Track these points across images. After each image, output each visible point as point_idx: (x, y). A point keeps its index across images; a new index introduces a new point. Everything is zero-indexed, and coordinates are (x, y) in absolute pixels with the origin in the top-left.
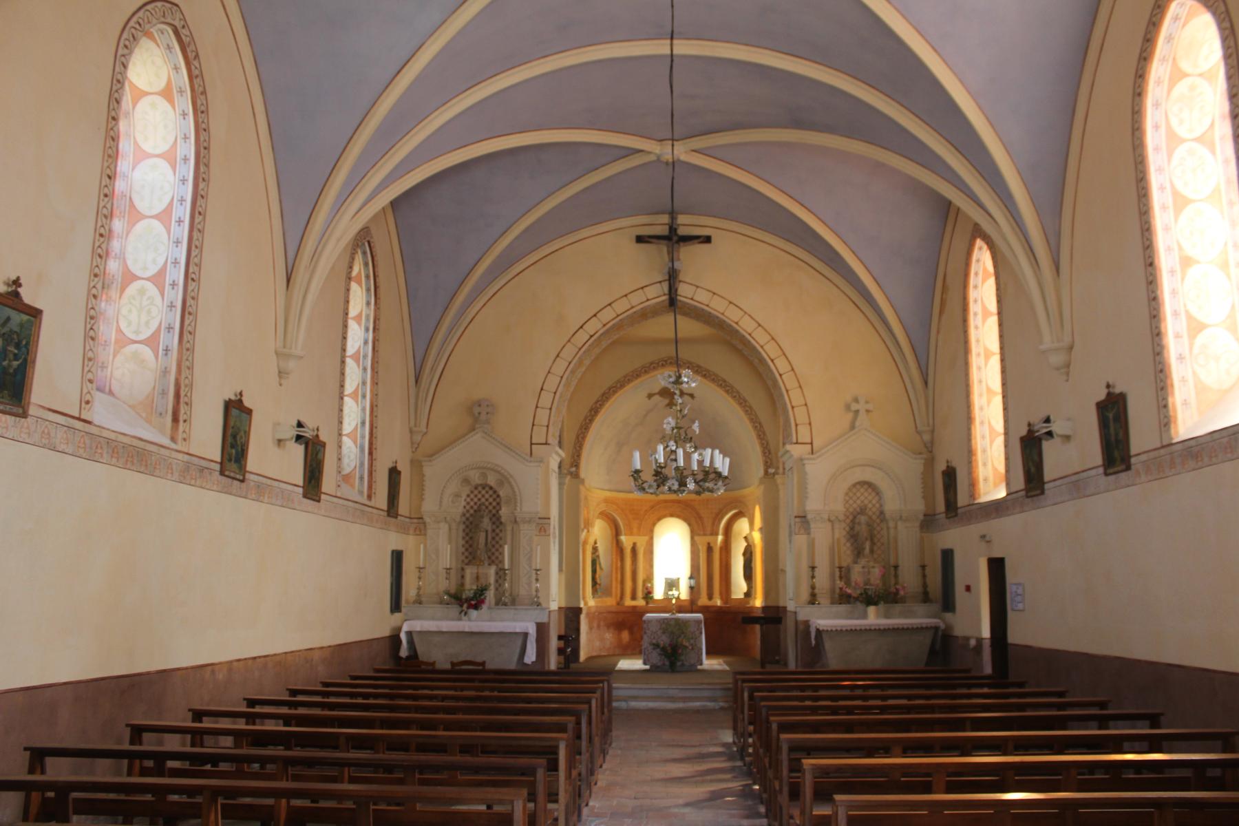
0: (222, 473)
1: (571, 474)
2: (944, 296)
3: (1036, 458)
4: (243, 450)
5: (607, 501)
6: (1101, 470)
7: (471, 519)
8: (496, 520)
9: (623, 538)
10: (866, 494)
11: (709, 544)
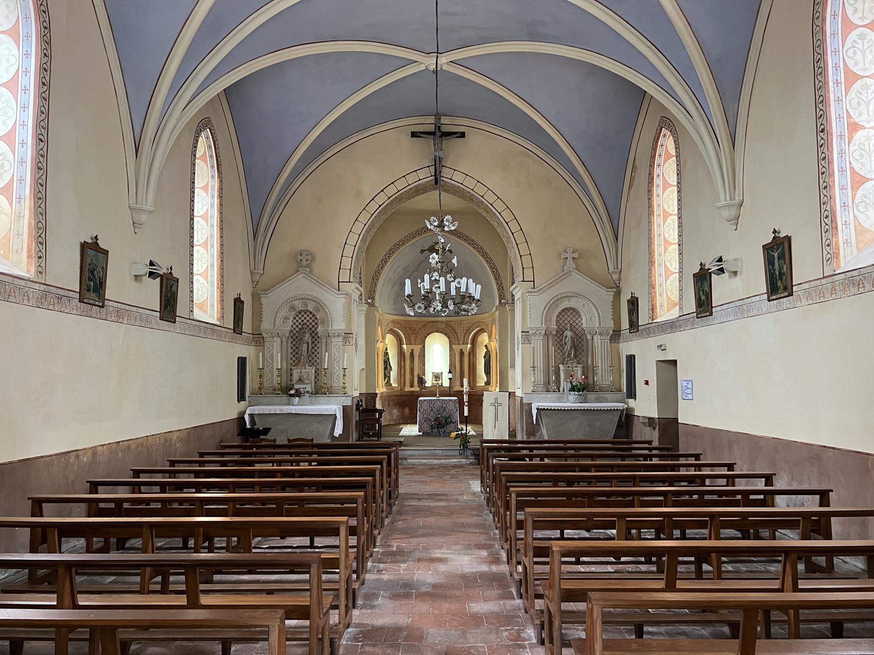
0: (81, 301)
1: (369, 303)
2: (633, 174)
3: (707, 289)
4: (101, 283)
5: (393, 322)
6: (766, 296)
7: (297, 334)
8: (314, 335)
9: (405, 346)
10: (572, 316)
11: (461, 350)
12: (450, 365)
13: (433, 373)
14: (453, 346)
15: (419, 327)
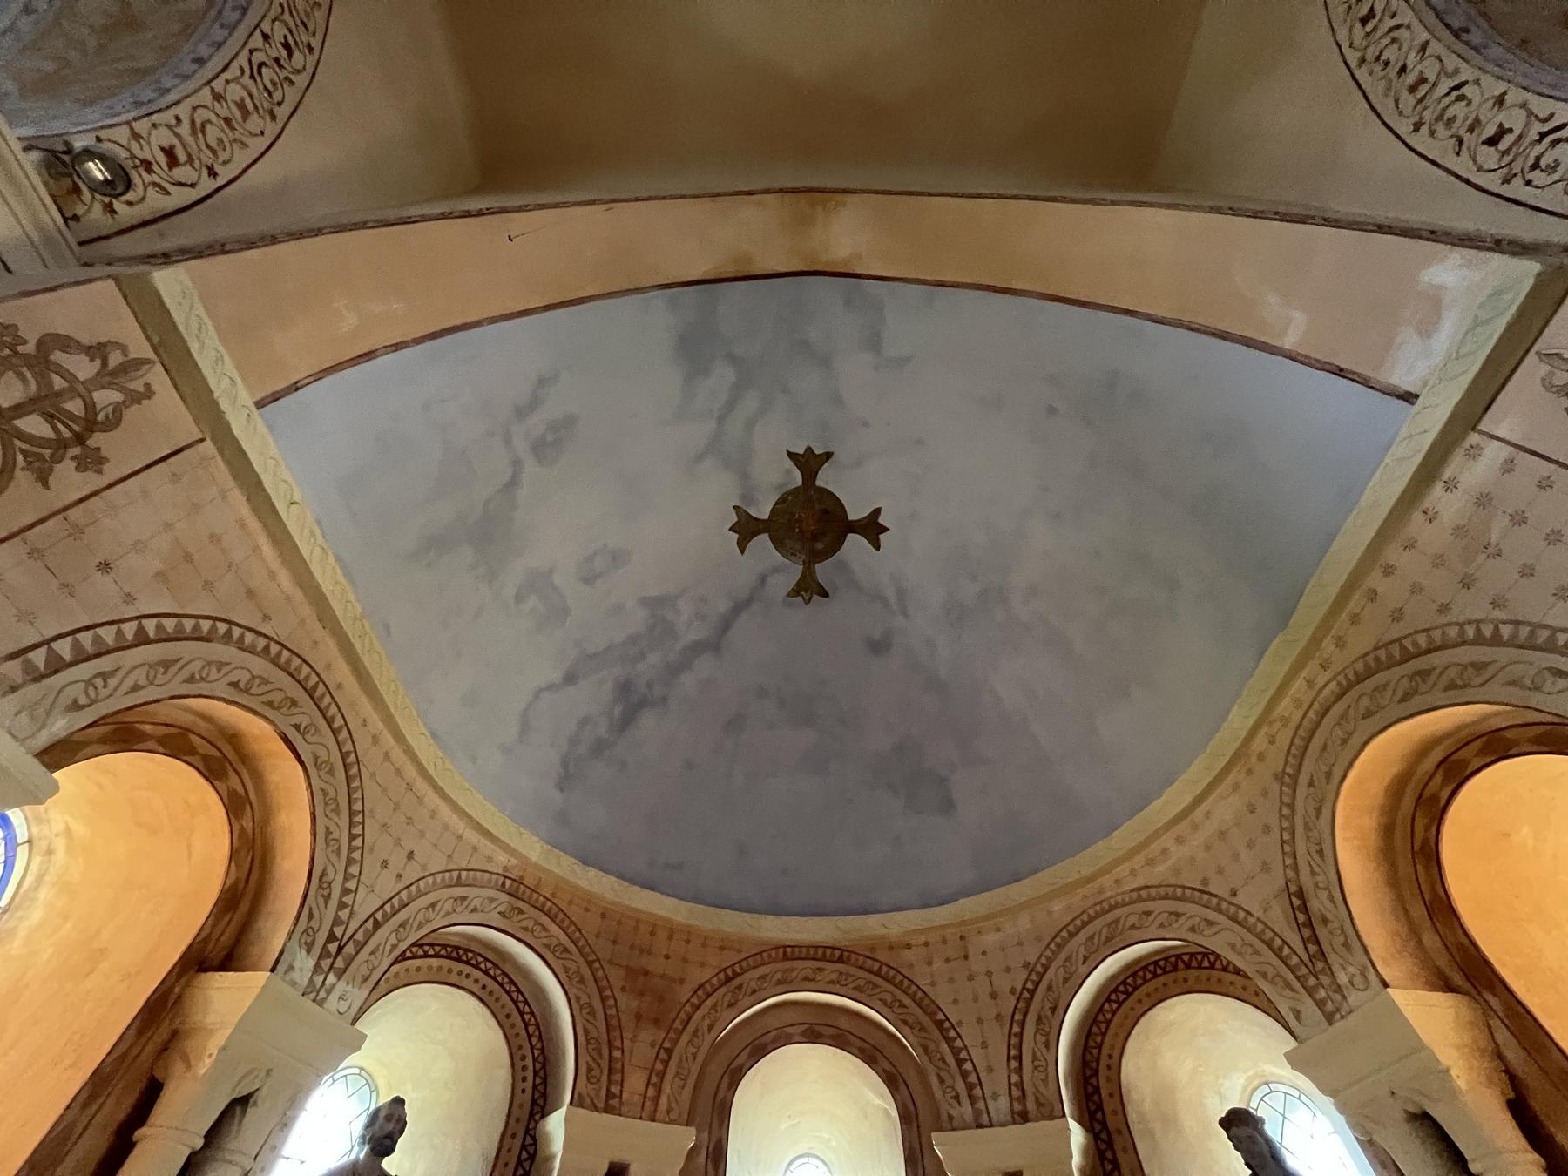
9: (556, 1125)
15: (698, 976)
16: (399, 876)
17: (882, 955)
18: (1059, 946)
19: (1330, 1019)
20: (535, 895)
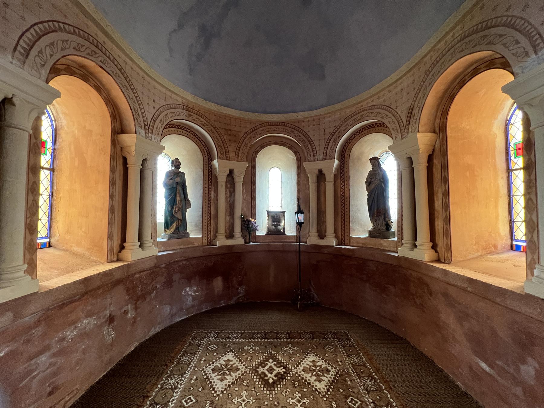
5: (188, 108)
9: (215, 162)
11: (320, 171)
12: (299, 199)
13: (269, 213)
14: (305, 165)
15: (244, 130)
16: (154, 107)
17: (295, 124)
18: (345, 122)
19: (402, 139)
20: (194, 110)
